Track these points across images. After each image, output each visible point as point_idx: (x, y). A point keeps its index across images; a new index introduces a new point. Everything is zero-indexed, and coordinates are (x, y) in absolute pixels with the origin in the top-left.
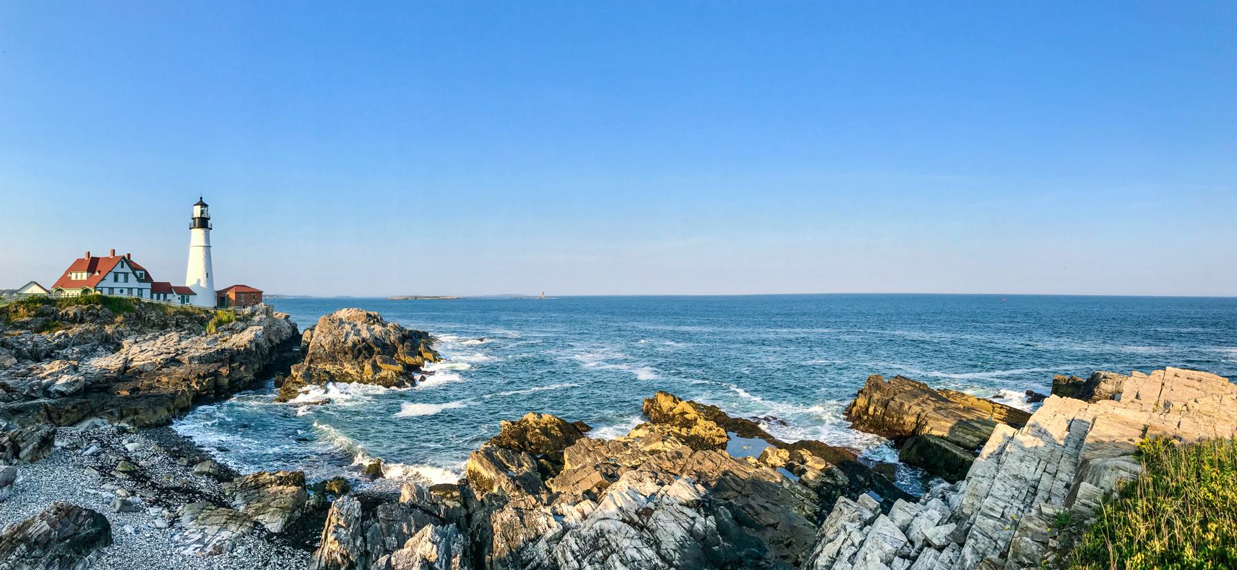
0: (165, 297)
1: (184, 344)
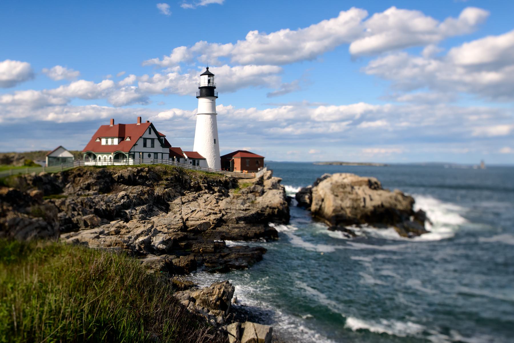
1: (222, 204)
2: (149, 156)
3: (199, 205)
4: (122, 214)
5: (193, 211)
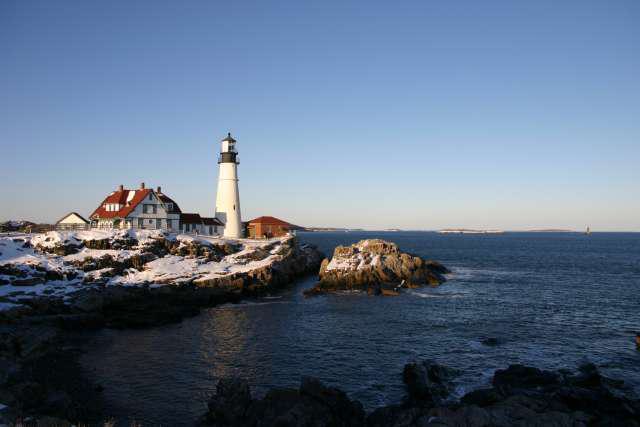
0: (194, 227)
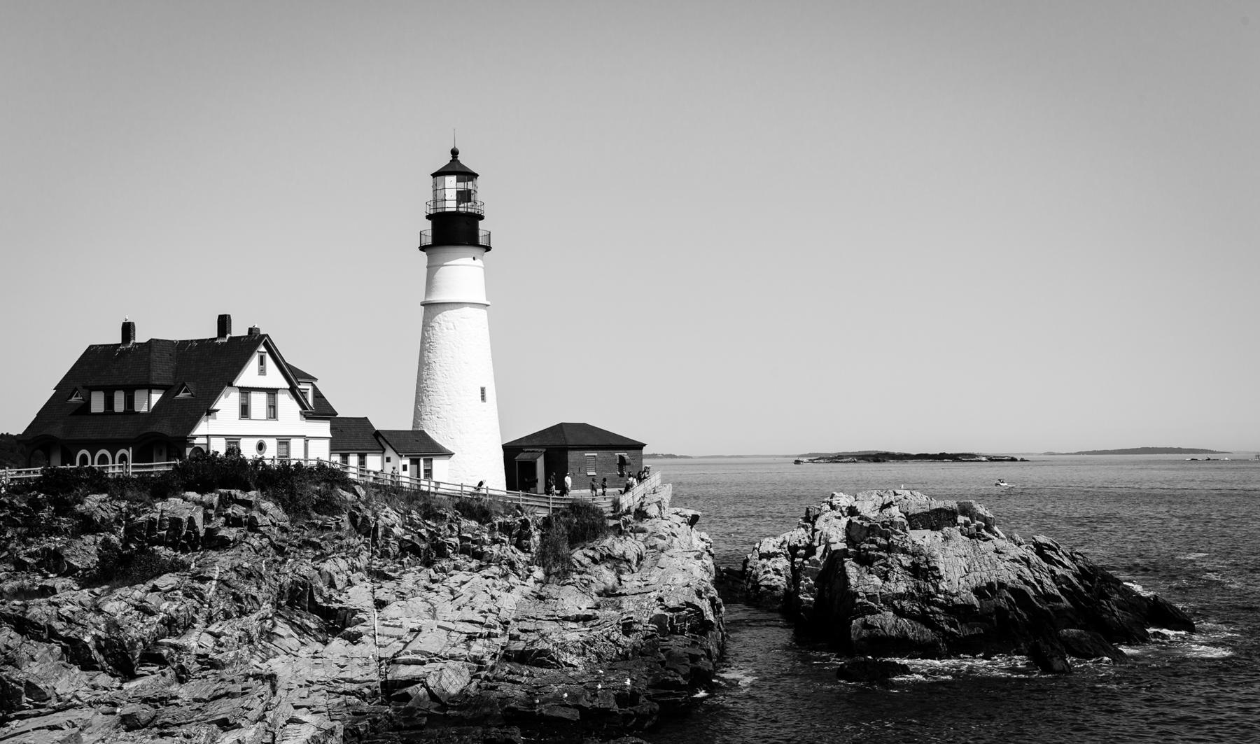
0: (362, 462)
2: (261, 447)
3: (433, 612)
4: (165, 652)
5: (412, 630)
